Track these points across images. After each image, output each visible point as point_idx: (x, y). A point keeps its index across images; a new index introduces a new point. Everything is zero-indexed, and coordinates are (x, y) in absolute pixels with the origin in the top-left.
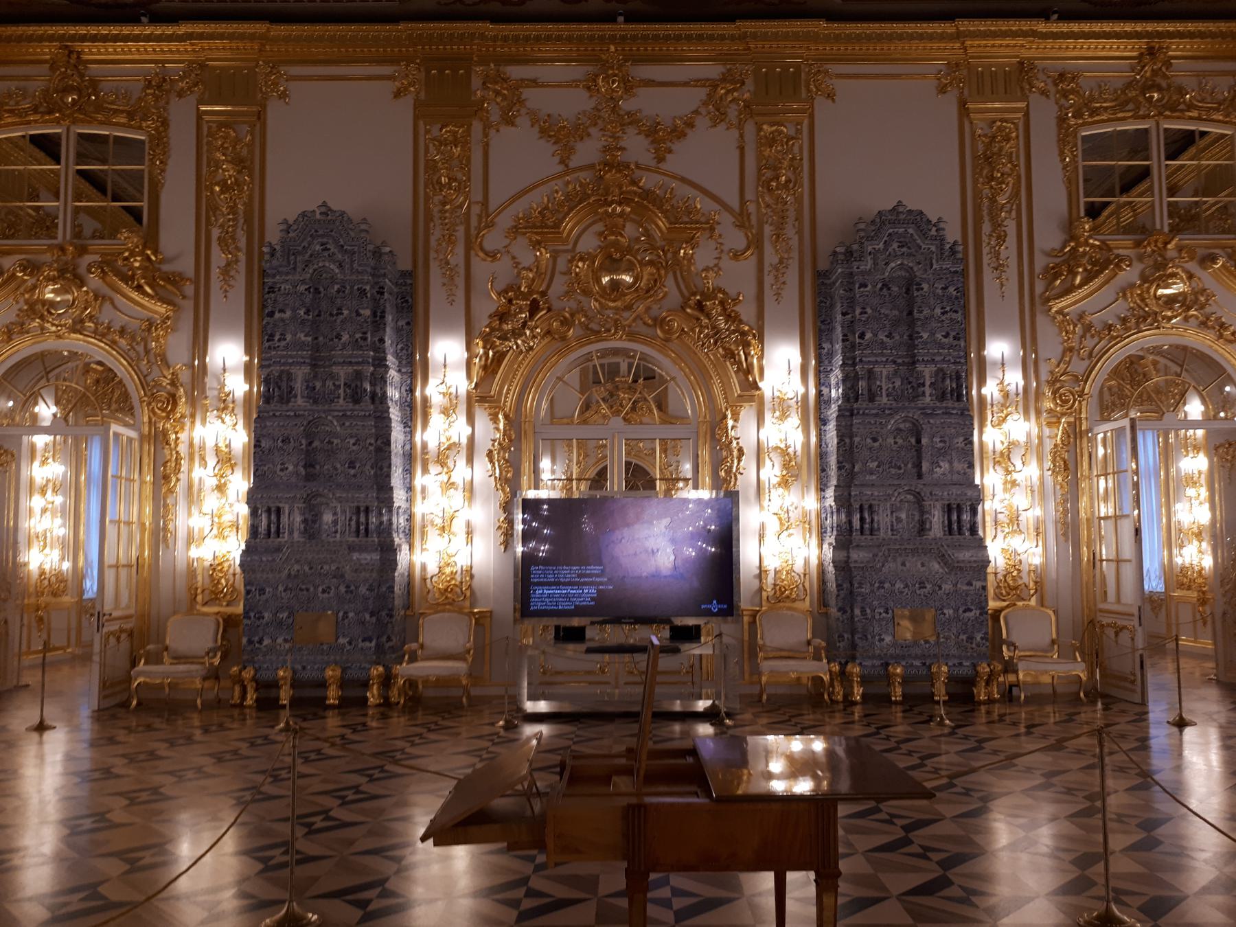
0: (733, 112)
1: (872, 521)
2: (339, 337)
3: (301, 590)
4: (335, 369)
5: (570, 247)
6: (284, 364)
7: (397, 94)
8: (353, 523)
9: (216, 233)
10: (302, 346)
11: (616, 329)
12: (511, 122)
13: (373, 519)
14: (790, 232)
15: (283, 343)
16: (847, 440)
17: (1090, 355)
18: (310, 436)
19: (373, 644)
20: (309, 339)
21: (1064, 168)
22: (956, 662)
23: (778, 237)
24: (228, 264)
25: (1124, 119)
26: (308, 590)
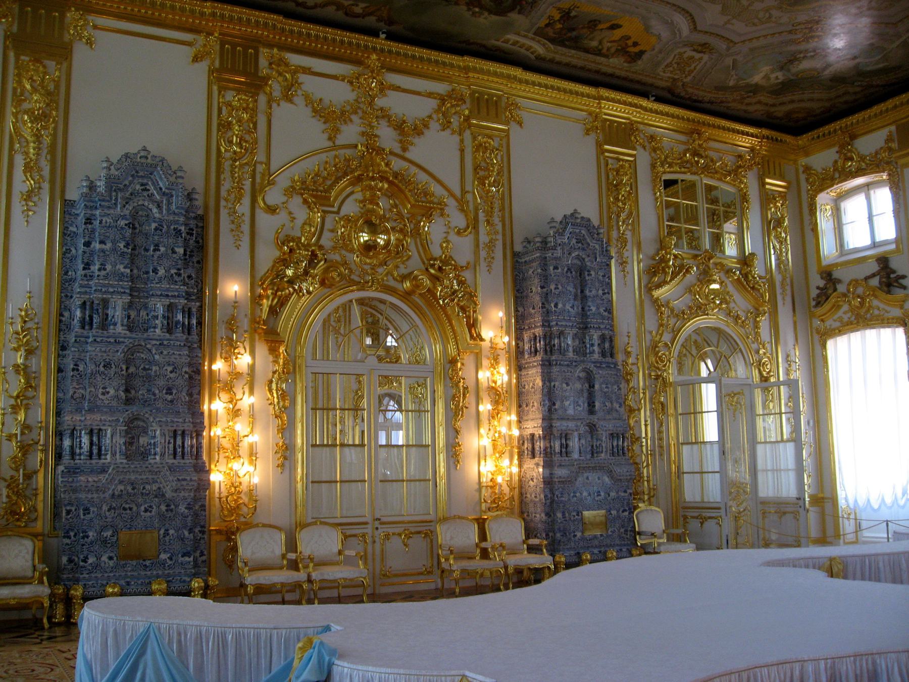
1: (567, 445)
2: (155, 271)
3: (125, 509)
4: (152, 302)
5: (335, 209)
7: (196, 59)
8: (171, 446)
11: (373, 282)
12: (289, 99)
13: (188, 442)
14: (496, 220)
15: (103, 273)
16: (548, 384)
17: (673, 331)
18: (128, 362)
19: (192, 559)
21: (656, 199)
22: (618, 548)
23: (488, 222)
25: (684, 173)
26: (131, 509)
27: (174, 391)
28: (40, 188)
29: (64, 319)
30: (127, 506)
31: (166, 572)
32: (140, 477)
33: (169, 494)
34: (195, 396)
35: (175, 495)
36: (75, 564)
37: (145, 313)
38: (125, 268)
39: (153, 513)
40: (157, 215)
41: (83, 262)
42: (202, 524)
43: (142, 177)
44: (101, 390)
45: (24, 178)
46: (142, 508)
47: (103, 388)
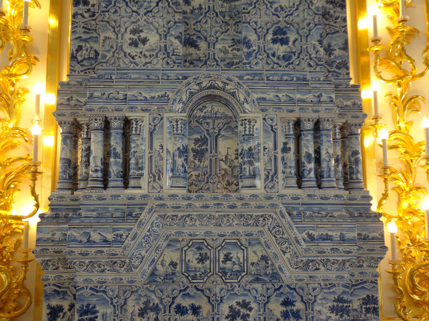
8: (291, 156)
26: (196, 310)
27: (292, 36)
30: (186, 303)
32: (216, 230)
33: (289, 275)
34: (337, 52)
35: (304, 275)
44: (128, 36)
47: (134, 32)
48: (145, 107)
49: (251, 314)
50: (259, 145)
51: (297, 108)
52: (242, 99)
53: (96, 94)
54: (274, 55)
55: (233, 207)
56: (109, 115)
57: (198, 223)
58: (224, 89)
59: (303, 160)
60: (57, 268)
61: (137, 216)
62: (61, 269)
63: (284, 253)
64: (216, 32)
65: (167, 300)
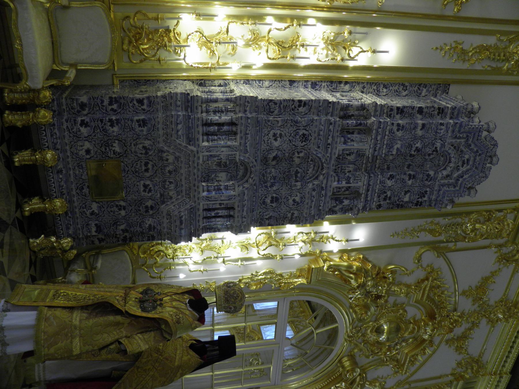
0: (459, 370)
2: (391, 177)
3: (146, 164)
6: (377, 132)
8: (218, 206)
9: (491, 40)
10: (390, 147)
11: (351, 337)
15: (395, 128)
19: (94, 234)
20: (394, 153)
24: (464, 52)
26: (147, 170)
27: (274, 205)
28: (464, 61)
29: (342, 85)
30: (150, 166)
31: (77, 210)
32: (183, 178)
34: (267, 222)
35: (164, 214)
36: (79, 112)
37: (351, 169)
38: (398, 149)
39: (143, 193)
40: (440, 175)
41: (404, 107)
42: (134, 238)
43: (475, 159)
45: (475, 45)
46: (148, 182)
47: (281, 135)
48: (242, 144)
49: (146, 193)
50: (223, 193)
51: (239, 209)
52: (244, 186)
53: (249, 121)
54: (266, 197)
55: (194, 185)
56: (239, 127)
57: (187, 170)
58: (250, 177)
59: (216, 211)
60: (162, 102)
61: (190, 145)
62: (162, 104)
63: (174, 206)
64: (280, 169)
65: (151, 158)
